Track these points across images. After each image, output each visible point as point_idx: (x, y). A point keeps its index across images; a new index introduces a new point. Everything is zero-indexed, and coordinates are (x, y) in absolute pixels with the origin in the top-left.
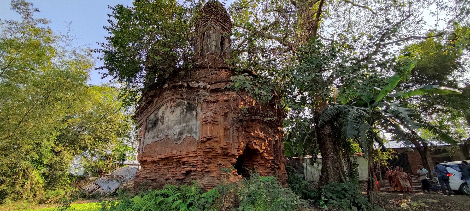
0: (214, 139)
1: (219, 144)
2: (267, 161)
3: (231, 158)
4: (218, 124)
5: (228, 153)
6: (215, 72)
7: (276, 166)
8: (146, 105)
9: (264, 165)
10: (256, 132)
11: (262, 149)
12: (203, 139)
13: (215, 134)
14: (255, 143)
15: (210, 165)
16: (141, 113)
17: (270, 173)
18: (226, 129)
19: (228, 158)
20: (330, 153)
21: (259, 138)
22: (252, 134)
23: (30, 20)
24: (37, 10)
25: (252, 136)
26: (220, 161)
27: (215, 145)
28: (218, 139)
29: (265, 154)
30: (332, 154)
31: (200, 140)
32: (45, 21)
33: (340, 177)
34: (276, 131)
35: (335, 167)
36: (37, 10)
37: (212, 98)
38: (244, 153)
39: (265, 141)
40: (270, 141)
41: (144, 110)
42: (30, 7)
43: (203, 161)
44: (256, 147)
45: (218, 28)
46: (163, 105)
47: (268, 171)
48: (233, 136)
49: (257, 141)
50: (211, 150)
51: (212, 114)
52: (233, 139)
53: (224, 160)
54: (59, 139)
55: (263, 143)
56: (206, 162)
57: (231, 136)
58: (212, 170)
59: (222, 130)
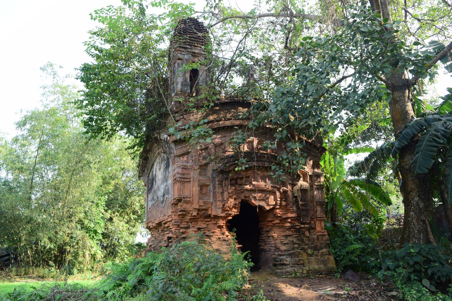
0: (186, 199)
1: (192, 205)
2: (284, 220)
3: (216, 220)
4: (190, 182)
5: (210, 214)
6: (182, 117)
7: (302, 226)
8: (144, 161)
9: (281, 225)
10: (254, 183)
11: (268, 205)
12: (174, 201)
13: (186, 193)
14: (255, 198)
15: (189, 230)
16: (143, 171)
17: (292, 235)
18: (202, 186)
19: (213, 220)
20: (413, 199)
21: (262, 191)
22: (248, 187)
23: (58, 79)
24: (60, 67)
25: (247, 190)
26: (202, 225)
27: (188, 207)
28: (191, 200)
29: (278, 211)
30: (417, 199)
31: (172, 202)
32: (70, 76)
33: (427, 235)
34: (295, 177)
35: (422, 221)
36: (60, 67)
37: (179, 151)
38: (240, 212)
39: (274, 193)
40: (285, 192)
41: (145, 168)
42: (55, 67)
43: (179, 225)
44: (257, 203)
45: (186, 57)
46: (155, 161)
47: (288, 233)
48: (214, 193)
49: (258, 195)
50: (185, 213)
51: (180, 170)
52: (215, 197)
53: (207, 223)
54: (109, 205)
55: (272, 197)
56: (183, 226)
57: (212, 193)
58: (190, 235)
59: (196, 189)
